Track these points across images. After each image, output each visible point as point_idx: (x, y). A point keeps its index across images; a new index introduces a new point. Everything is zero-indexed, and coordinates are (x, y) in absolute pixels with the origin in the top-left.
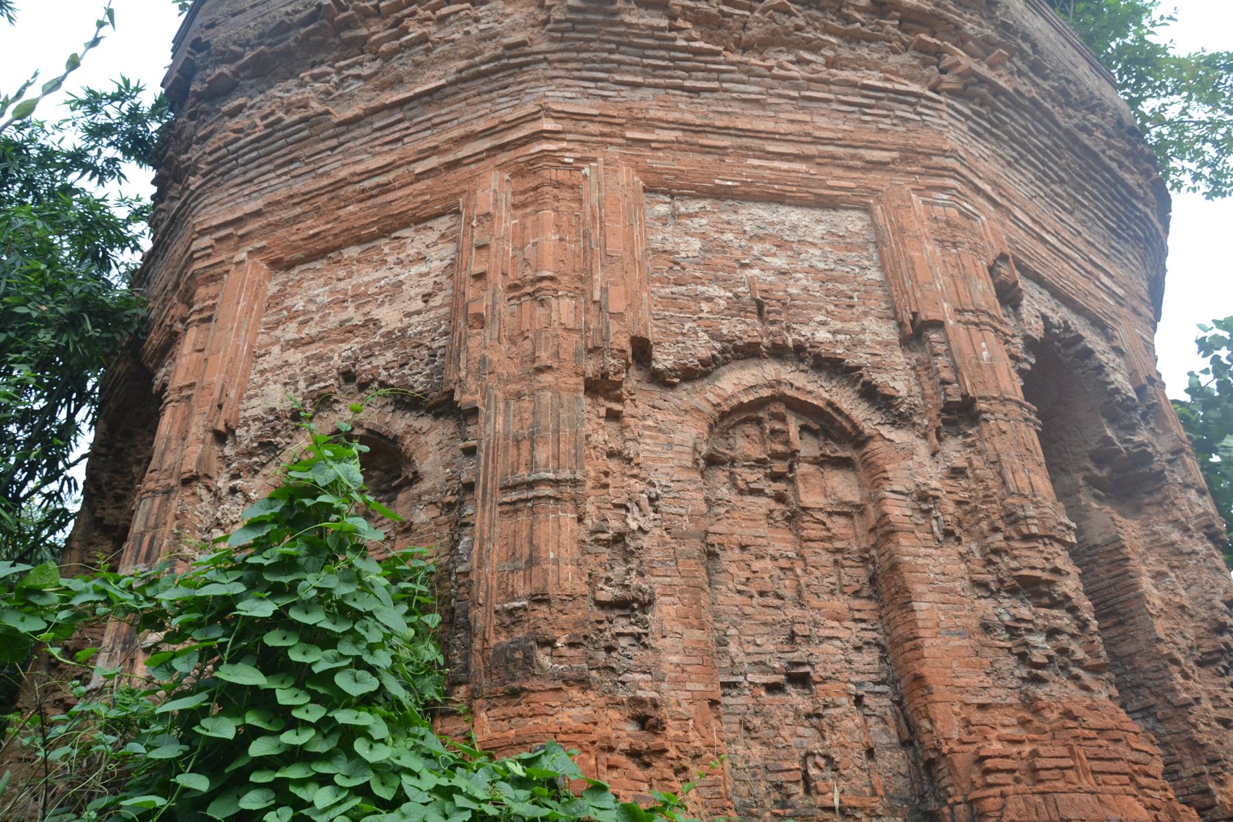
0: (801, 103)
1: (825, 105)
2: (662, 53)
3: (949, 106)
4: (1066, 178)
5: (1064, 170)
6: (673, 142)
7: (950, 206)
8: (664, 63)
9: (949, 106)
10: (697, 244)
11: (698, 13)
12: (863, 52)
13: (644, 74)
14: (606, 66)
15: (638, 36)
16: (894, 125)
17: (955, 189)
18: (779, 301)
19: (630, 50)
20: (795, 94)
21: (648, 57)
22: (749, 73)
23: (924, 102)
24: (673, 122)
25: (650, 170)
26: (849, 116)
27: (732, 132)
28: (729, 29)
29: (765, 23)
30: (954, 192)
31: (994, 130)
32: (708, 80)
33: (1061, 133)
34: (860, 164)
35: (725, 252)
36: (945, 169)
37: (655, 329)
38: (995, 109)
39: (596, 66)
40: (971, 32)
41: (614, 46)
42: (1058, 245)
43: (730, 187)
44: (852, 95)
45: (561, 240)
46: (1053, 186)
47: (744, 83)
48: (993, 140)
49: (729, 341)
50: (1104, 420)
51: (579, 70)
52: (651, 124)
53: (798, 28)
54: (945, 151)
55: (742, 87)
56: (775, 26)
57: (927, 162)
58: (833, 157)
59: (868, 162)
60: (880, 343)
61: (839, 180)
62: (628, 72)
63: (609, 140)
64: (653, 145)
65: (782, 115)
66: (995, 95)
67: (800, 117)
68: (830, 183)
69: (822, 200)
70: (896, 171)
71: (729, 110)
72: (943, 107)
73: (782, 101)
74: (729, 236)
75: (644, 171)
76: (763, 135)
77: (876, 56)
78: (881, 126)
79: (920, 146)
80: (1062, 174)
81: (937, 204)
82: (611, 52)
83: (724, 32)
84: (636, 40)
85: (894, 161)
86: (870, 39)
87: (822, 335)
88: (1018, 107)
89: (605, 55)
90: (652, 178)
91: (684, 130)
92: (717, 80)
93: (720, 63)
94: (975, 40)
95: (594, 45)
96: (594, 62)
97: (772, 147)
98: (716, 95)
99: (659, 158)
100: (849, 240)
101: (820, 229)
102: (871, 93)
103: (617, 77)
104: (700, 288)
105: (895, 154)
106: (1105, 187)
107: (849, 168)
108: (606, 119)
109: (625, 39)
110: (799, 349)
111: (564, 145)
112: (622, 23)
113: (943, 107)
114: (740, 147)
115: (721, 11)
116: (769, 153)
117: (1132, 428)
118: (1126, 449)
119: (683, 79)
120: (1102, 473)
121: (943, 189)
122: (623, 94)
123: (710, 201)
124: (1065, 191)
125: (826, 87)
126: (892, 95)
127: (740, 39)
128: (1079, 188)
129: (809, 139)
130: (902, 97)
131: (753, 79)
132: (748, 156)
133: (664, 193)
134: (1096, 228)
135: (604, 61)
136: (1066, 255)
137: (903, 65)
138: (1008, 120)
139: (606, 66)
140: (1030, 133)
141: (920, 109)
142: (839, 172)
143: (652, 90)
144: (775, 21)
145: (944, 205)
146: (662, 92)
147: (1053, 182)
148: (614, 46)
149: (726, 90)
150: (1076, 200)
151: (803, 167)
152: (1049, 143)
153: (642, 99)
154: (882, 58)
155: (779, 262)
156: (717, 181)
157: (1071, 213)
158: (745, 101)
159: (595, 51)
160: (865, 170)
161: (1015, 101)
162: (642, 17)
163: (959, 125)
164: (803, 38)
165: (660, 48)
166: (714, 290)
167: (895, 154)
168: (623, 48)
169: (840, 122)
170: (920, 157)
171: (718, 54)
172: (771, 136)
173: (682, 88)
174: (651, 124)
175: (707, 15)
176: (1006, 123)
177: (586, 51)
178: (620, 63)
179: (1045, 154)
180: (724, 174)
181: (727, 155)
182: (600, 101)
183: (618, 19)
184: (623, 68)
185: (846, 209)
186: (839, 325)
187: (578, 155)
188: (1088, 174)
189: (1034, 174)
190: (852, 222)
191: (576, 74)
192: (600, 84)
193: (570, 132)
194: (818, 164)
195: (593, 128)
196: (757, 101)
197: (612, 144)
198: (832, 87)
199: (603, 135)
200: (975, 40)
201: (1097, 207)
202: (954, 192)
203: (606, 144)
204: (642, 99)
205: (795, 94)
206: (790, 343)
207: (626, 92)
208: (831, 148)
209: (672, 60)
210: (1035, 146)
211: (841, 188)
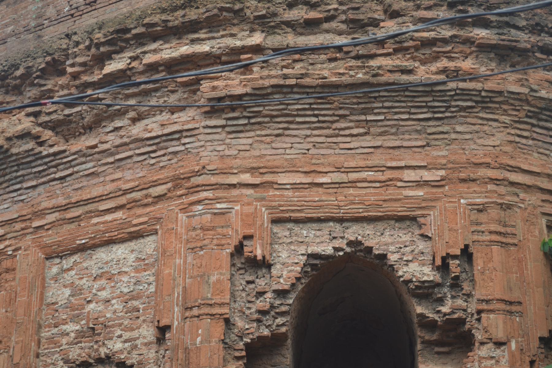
0: (117, 165)
1: (129, 161)
2: (39, 162)
3: (204, 127)
4: (347, 112)
5: (341, 108)
6: (54, 222)
7: (204, 213)
8: (41, 168)
9: (204, 127)
10: (68, 292)
11: (54, 122)
12: (153, 102)
13: (36, 177)
14: (18, 180)
15: (23, 158)
16: (169, 160)
17: (206, 199)
18: (102, 324)
19: (24, 166)
20: (111, 160)
21: (34, 167)
22: (84, 155)
23: (185, 134)
24: (52, 208)
25: (46, 246)
26: (144, 163)
27: (82, 203)
28: (75, 122)
29: (90, 111)
30: (207, 202)
31: (253, 121)
32: (67, 169)
33: (318, 90)
34: (150, 200)
35: (81, 294)
36: (198, 186)
37: (41, 363)
38: (245, 108)
39: (14, 182)
40: (219, 52)
41: (16, 168)
42: (343, 177)
43: (84, 243)
44: (143, 147)
45: (6, 311)
46: (335, 126)
47: (84, 163)
48: (257, 127)
49: (74, 362)
50: (414, 301)
51: (8, 187)
52: (40, 214)
53: (109, 106)
54: (197, 172)
55: (84, 166)
56: (95, 111)
57: (187, 185)
58: (135, 201)
59: (155, 197)
60: (146, 344)
61: (139, 217)
62: (29, 180)
63: (25, 231)
64: (46, 227)
65: (108, 178)
66: (241, 100)
67: (116, 176)
68: (134, 222)
69: (133, 235)
70: (171, 198)
71: (81, 185)
72: (202, 130)
73: (106, 167)
74: (84, 281)
75: (43, 247)
76: (97, 200)
77: (161, 101)
78: (161, 164)
79: (182, 174)
80: (341, 112)
81: (196, 215)
82: (17, 171)
83: (73, 125)
84: (24, 161)
85: (169, 190)
86: (156, 90)
87: (119, 346)
88: (264, 96)
89: (14, 174)
90: (48, 250)
91: (59, 211)
92: (71, 167)
93: (68, 157)
94: (225, 55)
95: (8, 171)
96: (12, 180)
97: (104, 206)
98: (73, 177)
99: (50, 236)
100: (147, 262)
101: (132, 257)
102: (151, 142)
103: (25, 185)
104: (64, 327)
105: (169, 185)
106: (397, 96)
107: (146, 205)
108: (21, 219)
109: (19, 162)
110: (108, 357)
111: (7, 243)
112: (12, 155)
113: (202, 130)
114: (87, 212)
115: (65, 115)
116: (102, 211)
117: (441, 301)
118: (439, 317)
119: (55, 173)
120: (435, 337)
121: (199, 202)
122: (30, 195)
123: (79, 254)
124: (351, 121)
125: (127, 147)
126: (164, 138)
127: (83, 125)
128: (365, 112)
129: (121, 193)
130: (170, 137)
131: (88, 158)
132: (92, 217)
133: (57, 257)
134: (402, 129)
135: (16, 177)
136: (350, 182)
137: (179, 100)
138: (261, 109)
139: (18, 180)
140: (288, 104)
141: (183, 142)
142: (140, 211)
143: (42, 187)
144: (93, 108)
145: (200, 215)
146: (48, 185)
147: (333, 122)
148: (16, 168)
149: (77, 172)
150: (367, 121)
151: (119, 215)
152: (312, 101)
153: (39, 195)
154: (165, 101)
155: (104, 294)
156: (78, 242)
157: (366, 134)
158: (87, 175)
159: (10, 173)
160: (154, 203)
161: (260, 94)
162: (20, 146)
163: (217, 137)
164: (115, 110)
165: (37, 159)
166: (71, 327)
167: (169, 185)
168: (21, 167)
169: (138, 171)
170: (184, 181)
171: (64, 151)
172: (100, 199)
173: (55, 179)
174: (40, 214)
175: (59, 121)
176: (260, 112)
177: (6, 174)
178: (23, 176)
179: (314, 109)
180: (80, 236)
181: (82, 220)
182: (21, 204)
183: (10, 153)
184: (26, 178)
185: (148, 236)
186: (127, 335)
187: (13, 248)
188: (371, 97)
189: (309, 128)
190: (149, 245)
191: (7, 190)
192: (19, 192)
193: (8, 233)
194: (128, 209)
195: (18, 226)
196: (93, 173)
197: (28, 234)
198: (131, 146)
199: (23, 229)
200: (225, 55)
201: (396, 113)
202: (207, 202)
203: (25, 235)
204: (39, 195)
205: (111, 160)
206: (103, 356)
207: (33, 193)
208: (134, 195)
209: (46, 164)
210: (298, 110)
211: (141, 224)
